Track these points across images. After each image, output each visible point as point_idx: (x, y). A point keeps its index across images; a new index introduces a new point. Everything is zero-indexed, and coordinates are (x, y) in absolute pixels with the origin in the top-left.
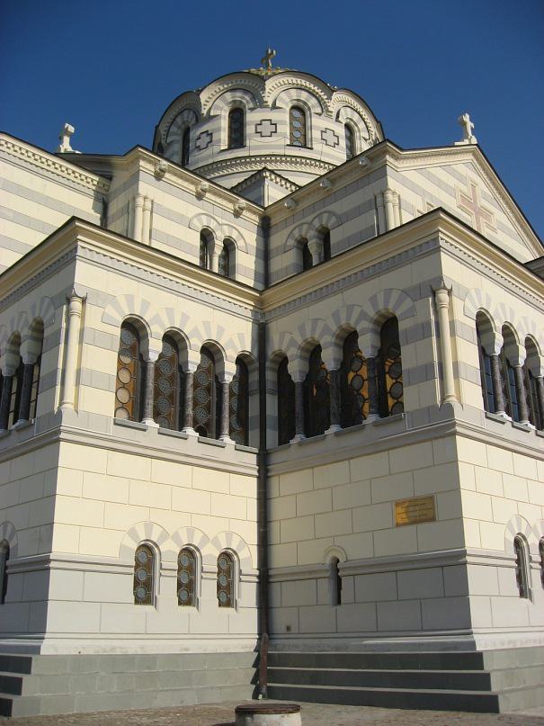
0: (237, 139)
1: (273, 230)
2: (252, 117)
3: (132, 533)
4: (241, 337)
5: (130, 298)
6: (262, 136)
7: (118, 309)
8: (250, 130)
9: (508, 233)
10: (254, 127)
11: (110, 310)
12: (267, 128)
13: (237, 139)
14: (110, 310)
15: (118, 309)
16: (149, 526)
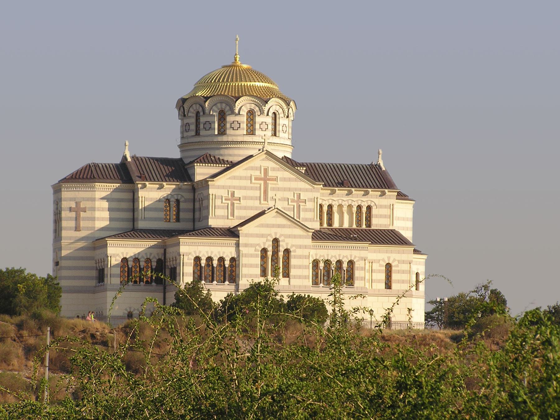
0: (197, 133)
1: (196, 191)
2: (203, 119)
3: (126, 310)
4: (158, 254)
5: (123, 253)
6: (206, 130)
7: (120, 257)
8: (201, 126)
9: (290, 180)
10: (203, 125)
11: (118, 258)
12: (207, 126)
13: (197, 133)
14: (118, 258)
15: (120, 257)
16: (130, 308)
